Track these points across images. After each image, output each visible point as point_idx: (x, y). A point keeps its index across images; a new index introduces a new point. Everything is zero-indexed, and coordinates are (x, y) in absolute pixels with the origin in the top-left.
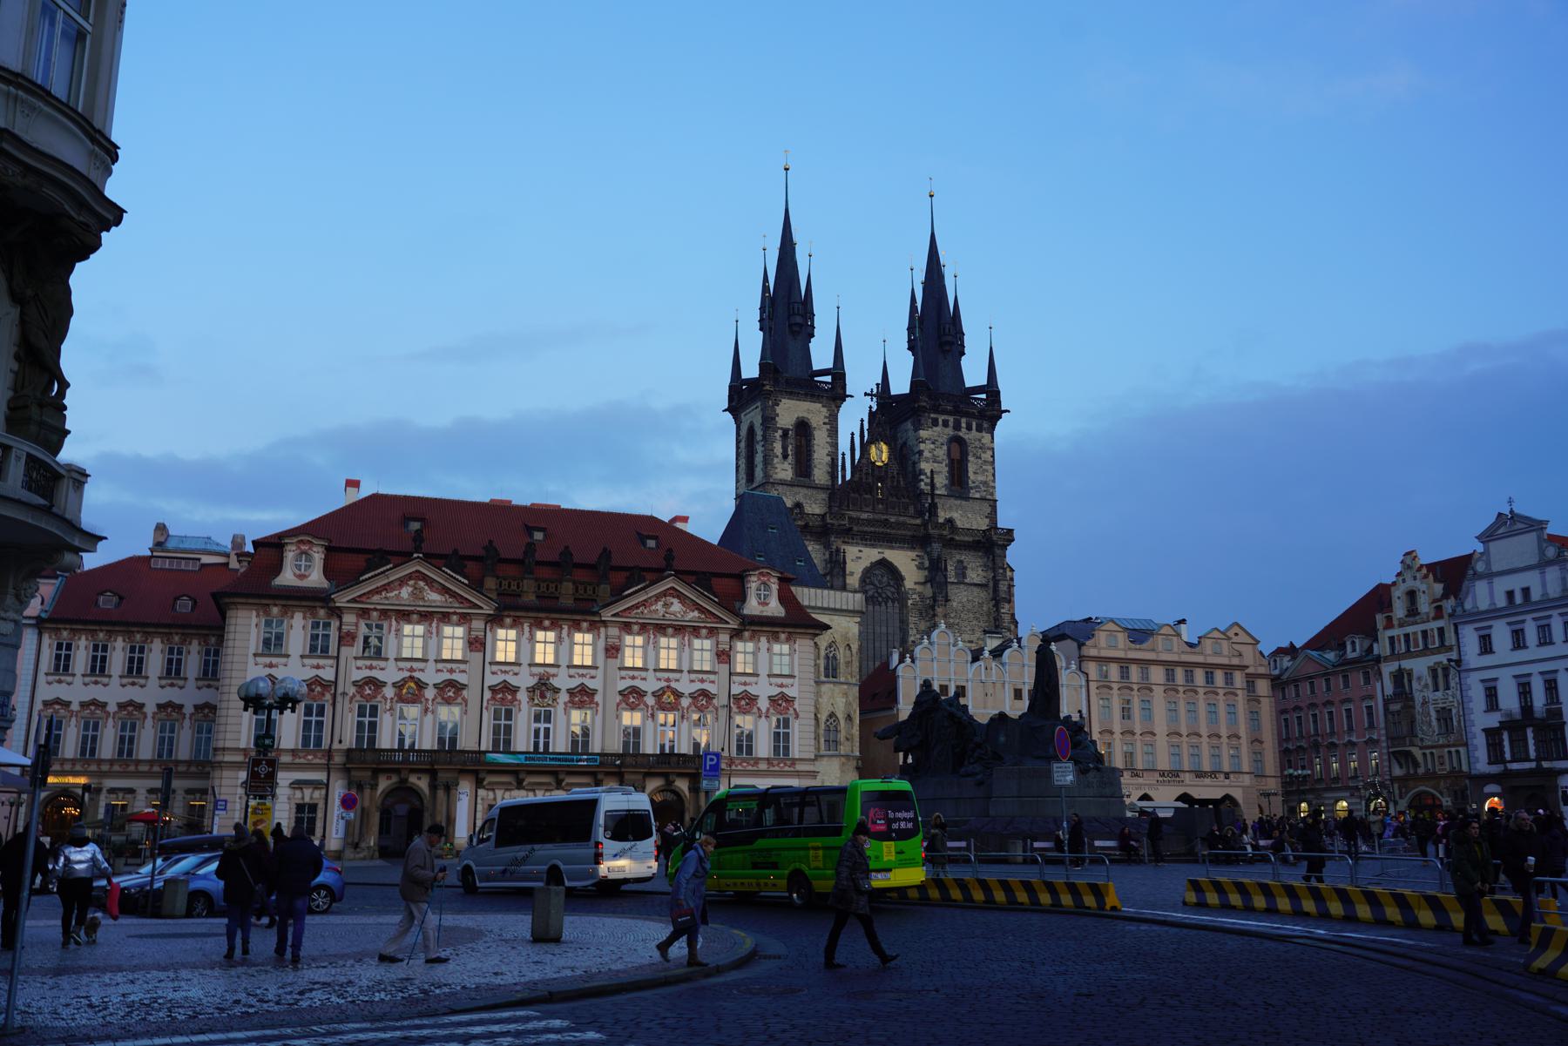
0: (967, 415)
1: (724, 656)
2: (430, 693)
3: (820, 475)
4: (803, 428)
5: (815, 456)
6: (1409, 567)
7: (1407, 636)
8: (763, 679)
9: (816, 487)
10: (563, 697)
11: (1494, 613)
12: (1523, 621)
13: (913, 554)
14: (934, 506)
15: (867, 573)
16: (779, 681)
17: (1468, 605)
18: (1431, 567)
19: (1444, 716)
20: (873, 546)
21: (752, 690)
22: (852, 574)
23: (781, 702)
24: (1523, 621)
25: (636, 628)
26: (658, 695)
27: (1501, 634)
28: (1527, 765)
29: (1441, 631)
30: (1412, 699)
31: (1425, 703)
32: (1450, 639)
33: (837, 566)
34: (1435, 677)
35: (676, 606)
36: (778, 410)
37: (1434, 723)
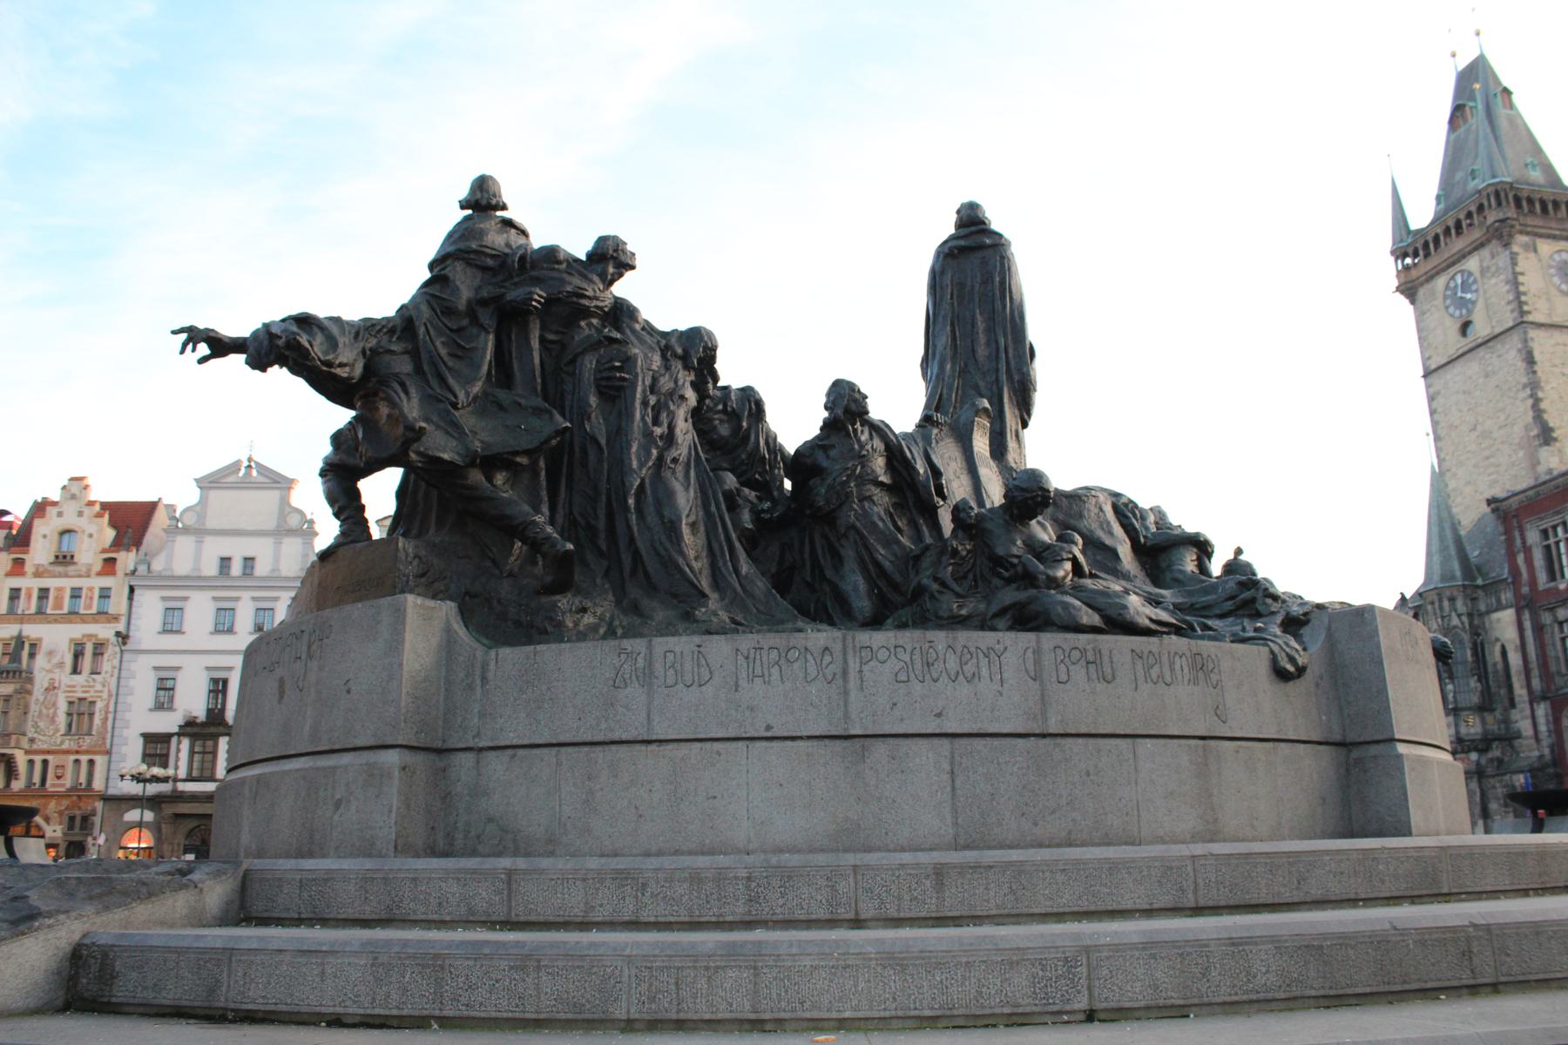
6: (73, 497)
7: (44, 593)
11: (196, 582)
12: (237, 599)
17: (157, 566)
18: (105, 506)
19: (80, 712)
24: (237, 599)
27: (200, 610)
28: (210, 787)
29: (105, 594)
30: (30, 680)
31: (52, 688)
32: (118, 604)
34: (78, 655)
37: (62, 719)
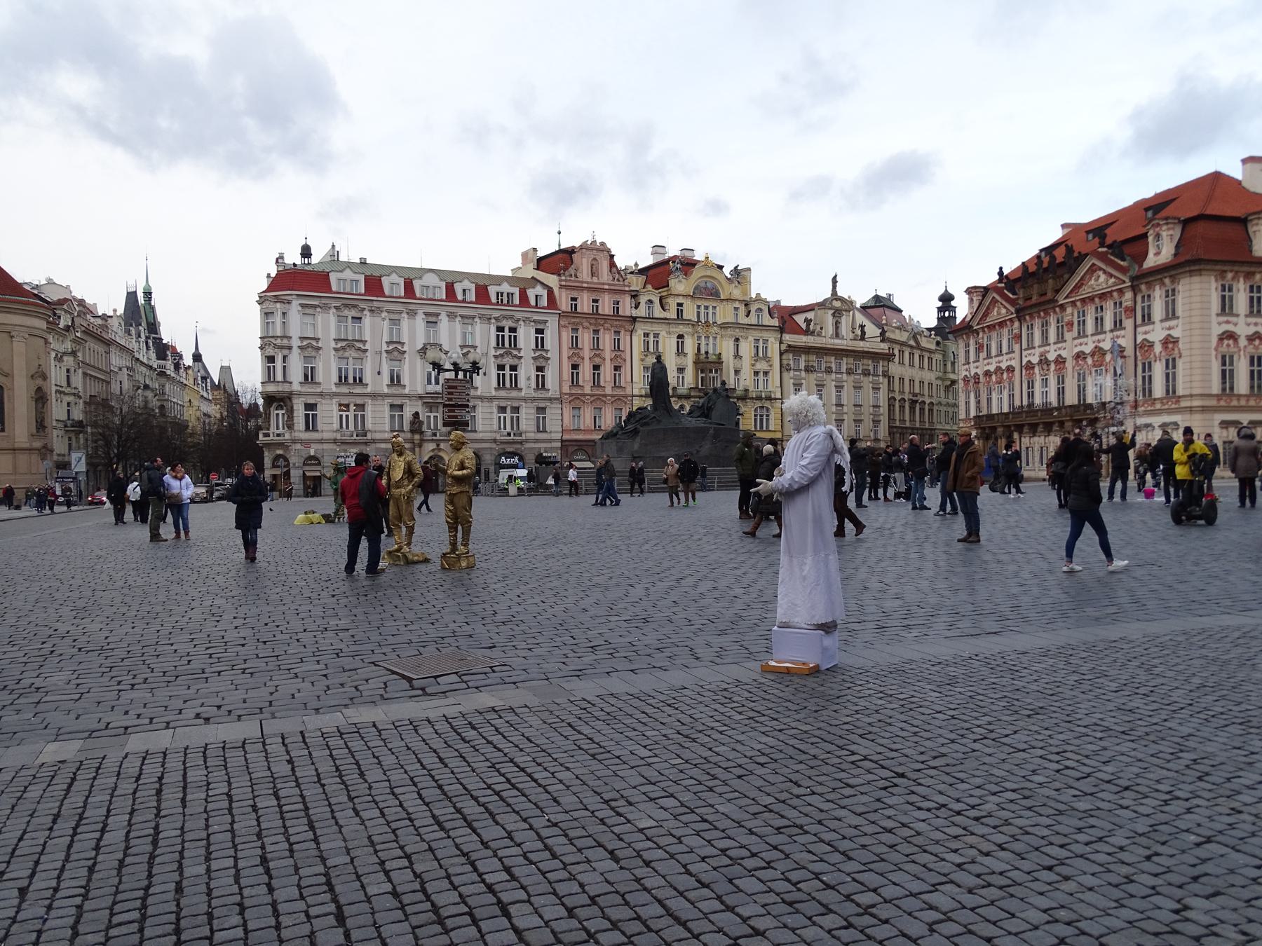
10: (1053, 367)
16: (1167, 324)
21: (1150, 337)
23: (1170, 342)
25: (1078, 304)
26: (1093, 354)
35: (1103, 277)
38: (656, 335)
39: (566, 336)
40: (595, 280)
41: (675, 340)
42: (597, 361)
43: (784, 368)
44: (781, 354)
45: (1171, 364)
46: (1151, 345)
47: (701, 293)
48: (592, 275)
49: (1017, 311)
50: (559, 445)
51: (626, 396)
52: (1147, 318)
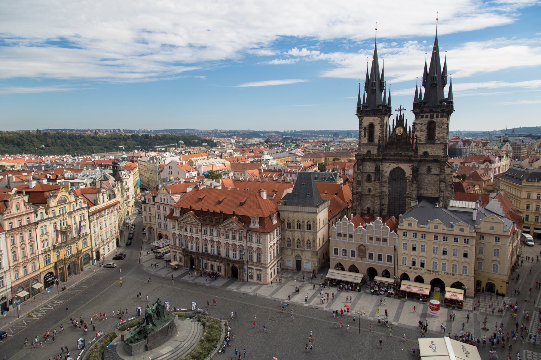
0: (436, 112)
1: (246, 238)
2: (194, 239)
3: (376, 140)
4: (371, 126)
5: (375, 134)
8: (254, 243)
9: (375, 145)
10: (215, 243)
13: (410, 165)
14: (416, 148)
15: (392, 172)
20: (394, 163)
22: (386, 172)
23: (258, 249)
26: (232, 245)
33: (378, 171)
35: (235, 225)
36: (363, 121)
38: (46, 226)
39: (9, 241)
40: (19, 211)
41: (52, 225)
42: (23, 246)
43: (90, 222)
44: (89, 216)
45: (259, 256)
46: (252, 248)
47: (60, 203)
48: (18, 209)
49: (202, 224)
50: (10, 290)
51: (36, 256)
52: (251, 240)
